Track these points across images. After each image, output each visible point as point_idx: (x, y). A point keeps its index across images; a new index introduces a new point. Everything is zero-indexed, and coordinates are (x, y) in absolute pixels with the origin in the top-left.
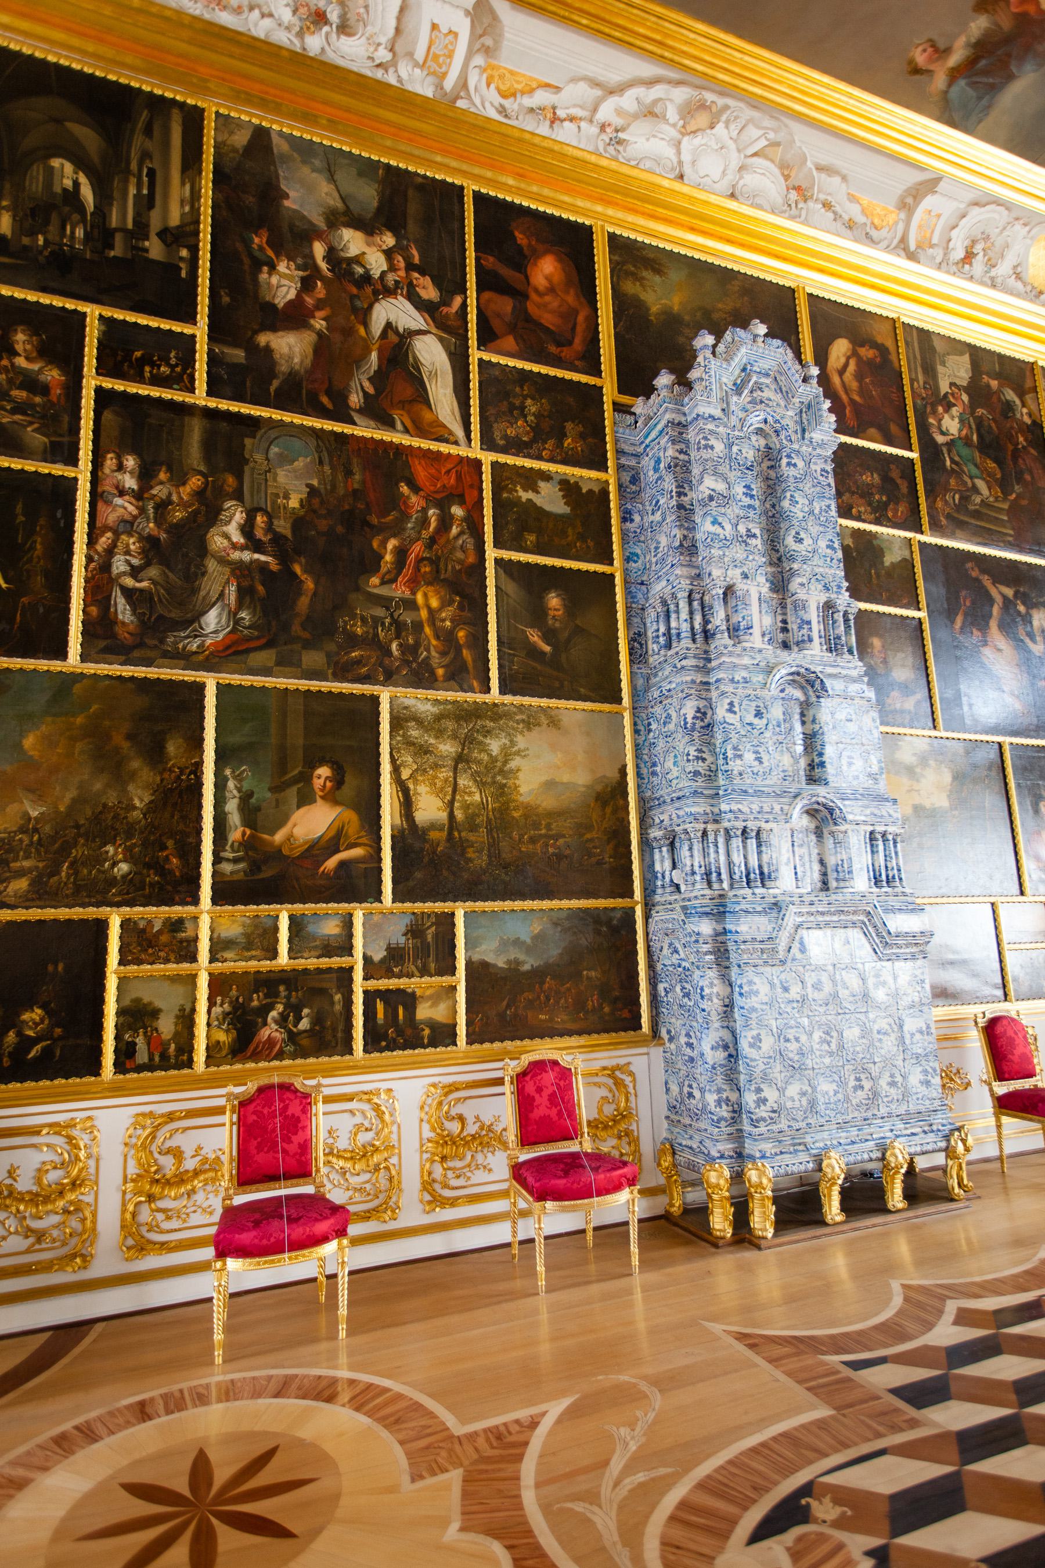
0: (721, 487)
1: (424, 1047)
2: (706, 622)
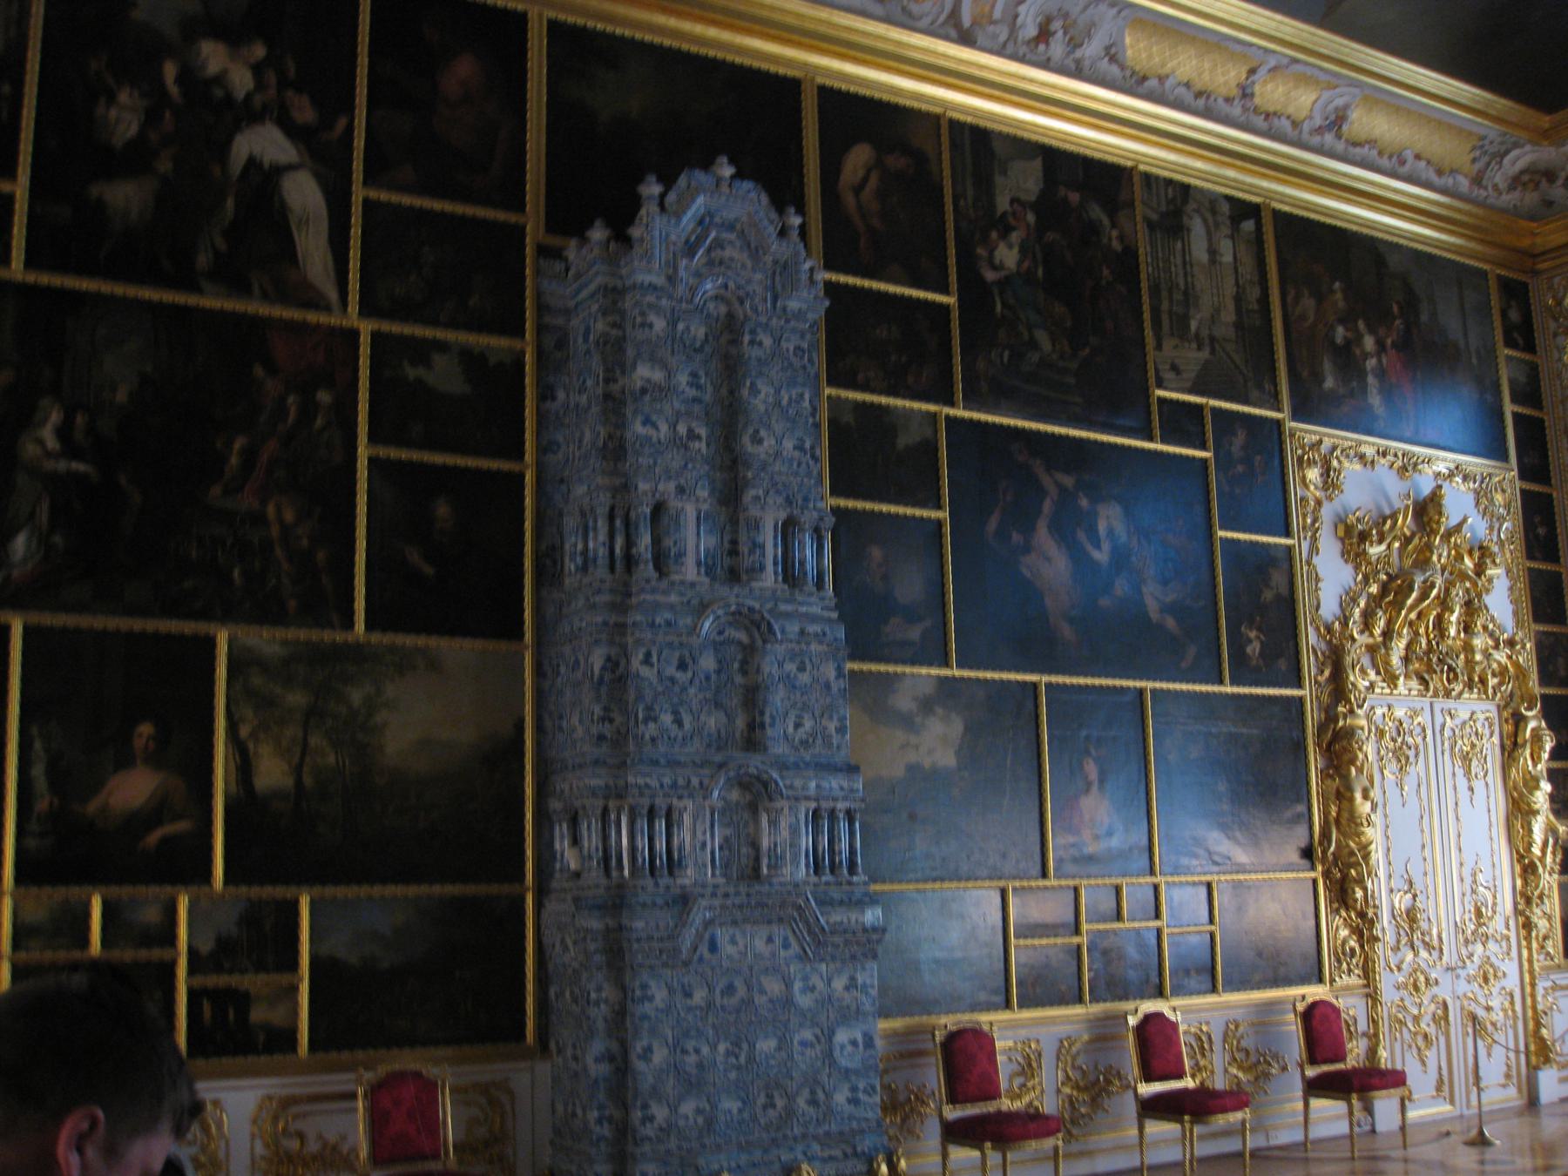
0: (658, 376)
1: (258, 1053)
2: (630, 543)
